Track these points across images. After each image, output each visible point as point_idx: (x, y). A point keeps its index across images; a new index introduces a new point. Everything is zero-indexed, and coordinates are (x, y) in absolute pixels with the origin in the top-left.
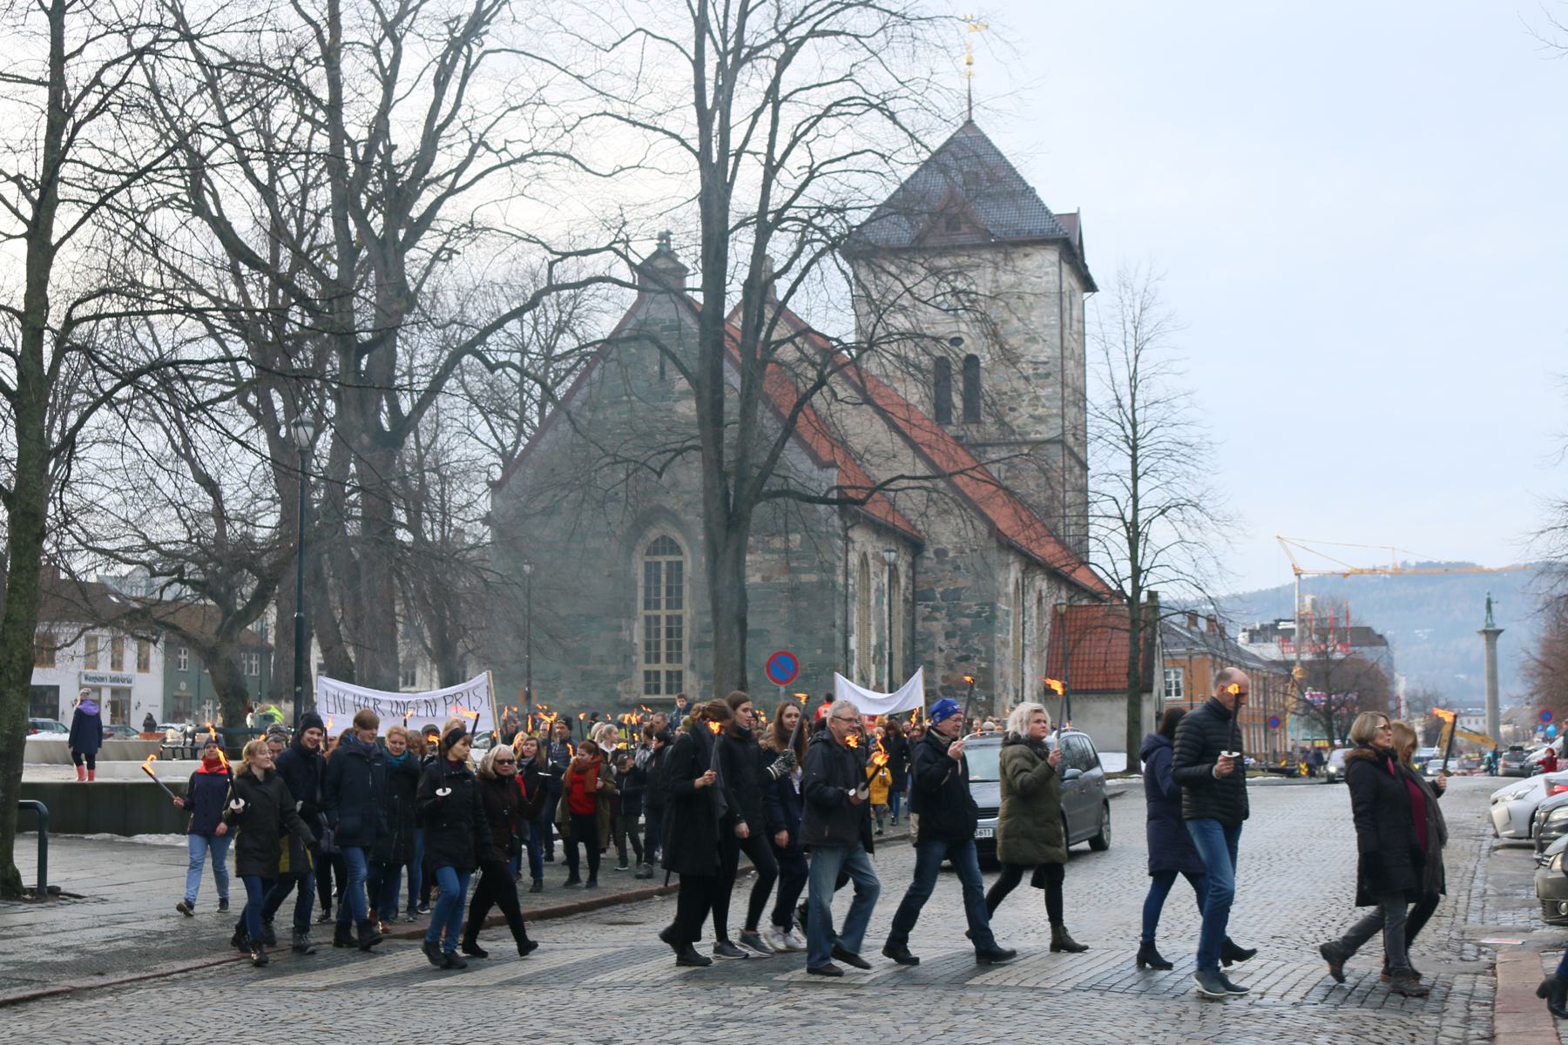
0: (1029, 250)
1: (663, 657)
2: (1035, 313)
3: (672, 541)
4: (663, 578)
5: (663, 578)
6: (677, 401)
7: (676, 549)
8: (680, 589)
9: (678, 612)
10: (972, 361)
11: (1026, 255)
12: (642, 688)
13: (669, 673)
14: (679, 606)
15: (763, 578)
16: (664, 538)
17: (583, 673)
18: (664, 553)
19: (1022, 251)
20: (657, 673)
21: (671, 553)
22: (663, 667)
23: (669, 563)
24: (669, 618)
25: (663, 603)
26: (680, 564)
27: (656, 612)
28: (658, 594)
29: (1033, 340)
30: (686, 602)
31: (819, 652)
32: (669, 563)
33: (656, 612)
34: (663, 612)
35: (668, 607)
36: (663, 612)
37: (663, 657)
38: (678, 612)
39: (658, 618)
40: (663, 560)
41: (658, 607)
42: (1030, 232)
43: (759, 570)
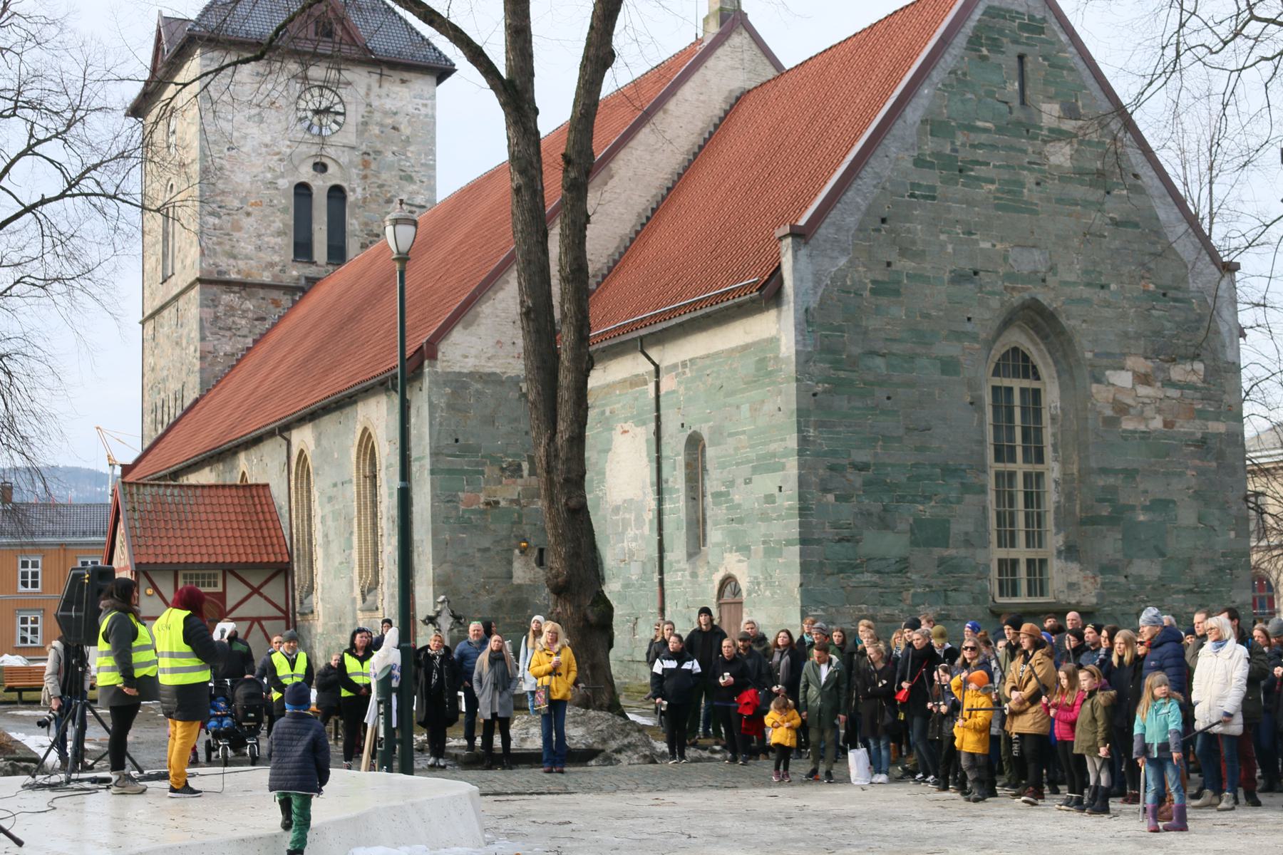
0: (406, 76)
1: (1021, 538)
2: (411, 148)
3: (1026, 358)
4: (1017, 413)
5: (1017, 413)
6: (1045, 142)
7: (1029, 370)
8: (1039, 431)
9: (1039, 468)
10: (337, 193)
11: (403, 81)
12: (996, 589)
13: (1030, 562)
14: (1040, 459)
15: (1166, 424)
16: (1015, 350)
17: (942, 561)
18: (1016, 375)
19: (397, 75)
20: (1015, 562)
21: (1026, 376)
22: (1021, 552)
23: (1023, 391)
24: (1027, 476)
25: (1019, 451)
26: (1037, 393)
27: (1010, 467)
28: (1011, 438)
29: (409, 179)
30: (1048, 453)
31: (1232, 534)
32: (1023, 391)
33: (1010, 467)
34: (1020, 467)
35: (1026, 460)
36: (1020, 467)
37: (1021, 538)
38: (1039, 468)
39: (1012, 475)
40: (1017, 384)
41: (1012, 459)
42: (400, 53)
43: (1159, 411)
